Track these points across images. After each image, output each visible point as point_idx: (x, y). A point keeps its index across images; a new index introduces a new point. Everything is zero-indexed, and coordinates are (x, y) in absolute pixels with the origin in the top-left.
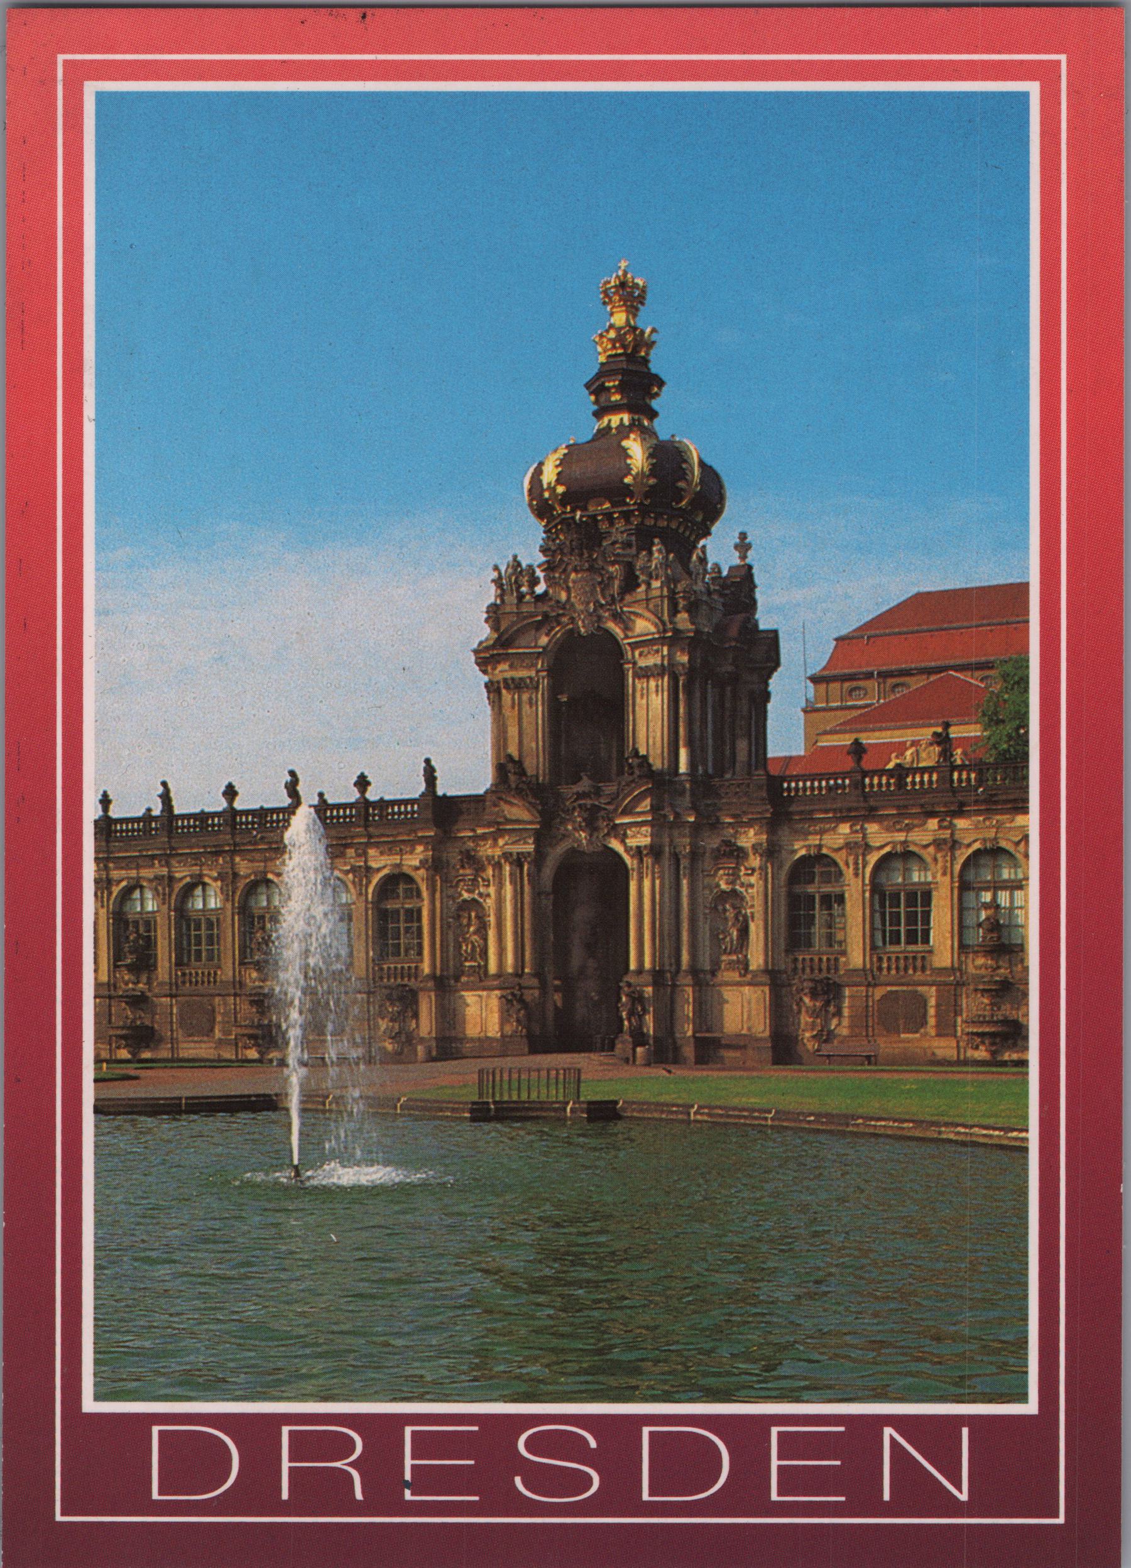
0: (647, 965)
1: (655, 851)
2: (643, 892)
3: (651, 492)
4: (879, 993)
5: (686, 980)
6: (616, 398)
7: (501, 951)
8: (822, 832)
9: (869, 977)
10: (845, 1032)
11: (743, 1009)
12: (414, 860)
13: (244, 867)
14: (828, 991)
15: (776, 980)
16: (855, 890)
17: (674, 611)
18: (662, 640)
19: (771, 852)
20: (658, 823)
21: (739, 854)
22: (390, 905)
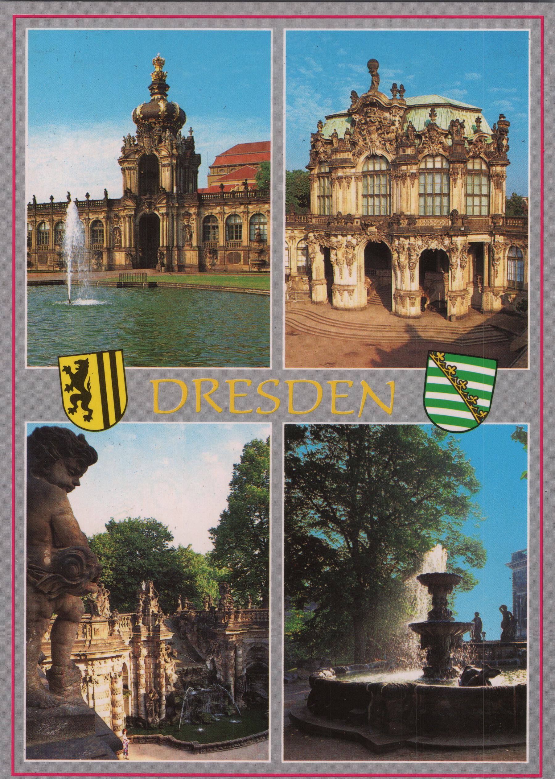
0: (165, 245)
1: (167, 214)
2: (164, 225)
3: (166, 117)
4: (228, 253)
5: (175, 249)
6: (156, 91)
7: (125, 242)
8: (212, 209)
9: (225, 248)
10: (219, 263)
11: (191, 257)
12: (102, 216)
13: (55, 218)
14: (214, 252)
15: (200, 249)
16: (221, 225)
17: (172, 149)
18: (169, 157)
19: (198, 214)
20: (168, 206)
21: (189, 215)
22: (95, 229)
